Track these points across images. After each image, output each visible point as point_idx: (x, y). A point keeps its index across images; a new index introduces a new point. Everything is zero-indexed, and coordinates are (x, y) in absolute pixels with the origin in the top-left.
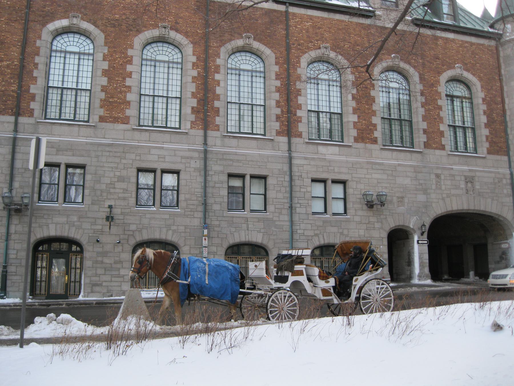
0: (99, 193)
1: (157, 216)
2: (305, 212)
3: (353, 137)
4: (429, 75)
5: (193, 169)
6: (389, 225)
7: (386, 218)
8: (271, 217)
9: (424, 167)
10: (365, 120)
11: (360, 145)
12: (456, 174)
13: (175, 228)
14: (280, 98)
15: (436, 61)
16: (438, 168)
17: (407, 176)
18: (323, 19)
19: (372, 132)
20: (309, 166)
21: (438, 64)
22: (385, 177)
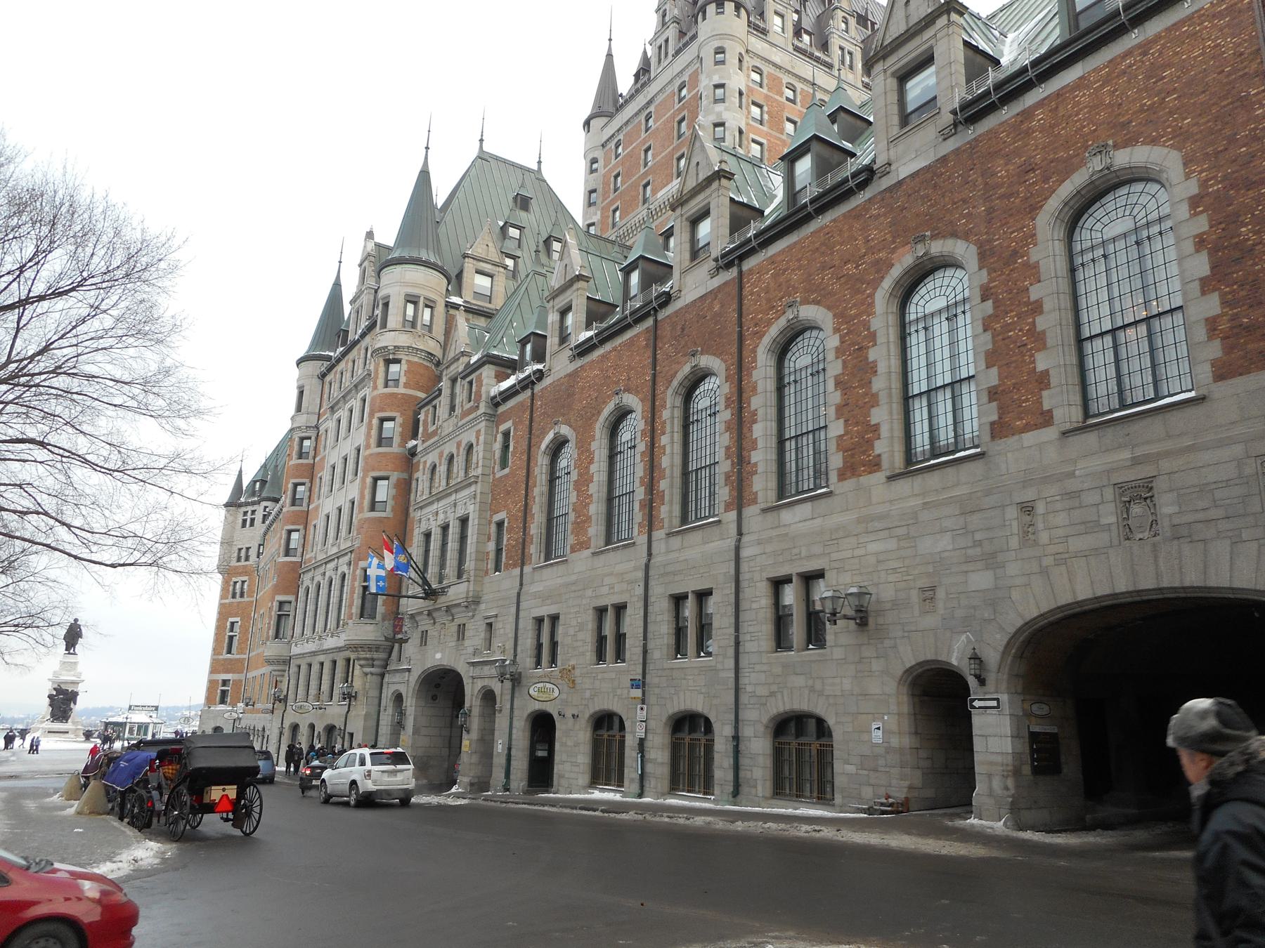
0: (566, 649)
1: (606, 675)
4: (1005, 233)
6: (903, 662)
7: (895, 647)
8: (713, 664)
9: (988, 493)
10: (857, 424)
11: (850, 484)
12: (1086, 486)
13: (619, 692)
15: (1025, 182)
16: (1026, 484)
17: (943, 531)
18: (790, 247)
19: (870, 444)
22: (892, 544)
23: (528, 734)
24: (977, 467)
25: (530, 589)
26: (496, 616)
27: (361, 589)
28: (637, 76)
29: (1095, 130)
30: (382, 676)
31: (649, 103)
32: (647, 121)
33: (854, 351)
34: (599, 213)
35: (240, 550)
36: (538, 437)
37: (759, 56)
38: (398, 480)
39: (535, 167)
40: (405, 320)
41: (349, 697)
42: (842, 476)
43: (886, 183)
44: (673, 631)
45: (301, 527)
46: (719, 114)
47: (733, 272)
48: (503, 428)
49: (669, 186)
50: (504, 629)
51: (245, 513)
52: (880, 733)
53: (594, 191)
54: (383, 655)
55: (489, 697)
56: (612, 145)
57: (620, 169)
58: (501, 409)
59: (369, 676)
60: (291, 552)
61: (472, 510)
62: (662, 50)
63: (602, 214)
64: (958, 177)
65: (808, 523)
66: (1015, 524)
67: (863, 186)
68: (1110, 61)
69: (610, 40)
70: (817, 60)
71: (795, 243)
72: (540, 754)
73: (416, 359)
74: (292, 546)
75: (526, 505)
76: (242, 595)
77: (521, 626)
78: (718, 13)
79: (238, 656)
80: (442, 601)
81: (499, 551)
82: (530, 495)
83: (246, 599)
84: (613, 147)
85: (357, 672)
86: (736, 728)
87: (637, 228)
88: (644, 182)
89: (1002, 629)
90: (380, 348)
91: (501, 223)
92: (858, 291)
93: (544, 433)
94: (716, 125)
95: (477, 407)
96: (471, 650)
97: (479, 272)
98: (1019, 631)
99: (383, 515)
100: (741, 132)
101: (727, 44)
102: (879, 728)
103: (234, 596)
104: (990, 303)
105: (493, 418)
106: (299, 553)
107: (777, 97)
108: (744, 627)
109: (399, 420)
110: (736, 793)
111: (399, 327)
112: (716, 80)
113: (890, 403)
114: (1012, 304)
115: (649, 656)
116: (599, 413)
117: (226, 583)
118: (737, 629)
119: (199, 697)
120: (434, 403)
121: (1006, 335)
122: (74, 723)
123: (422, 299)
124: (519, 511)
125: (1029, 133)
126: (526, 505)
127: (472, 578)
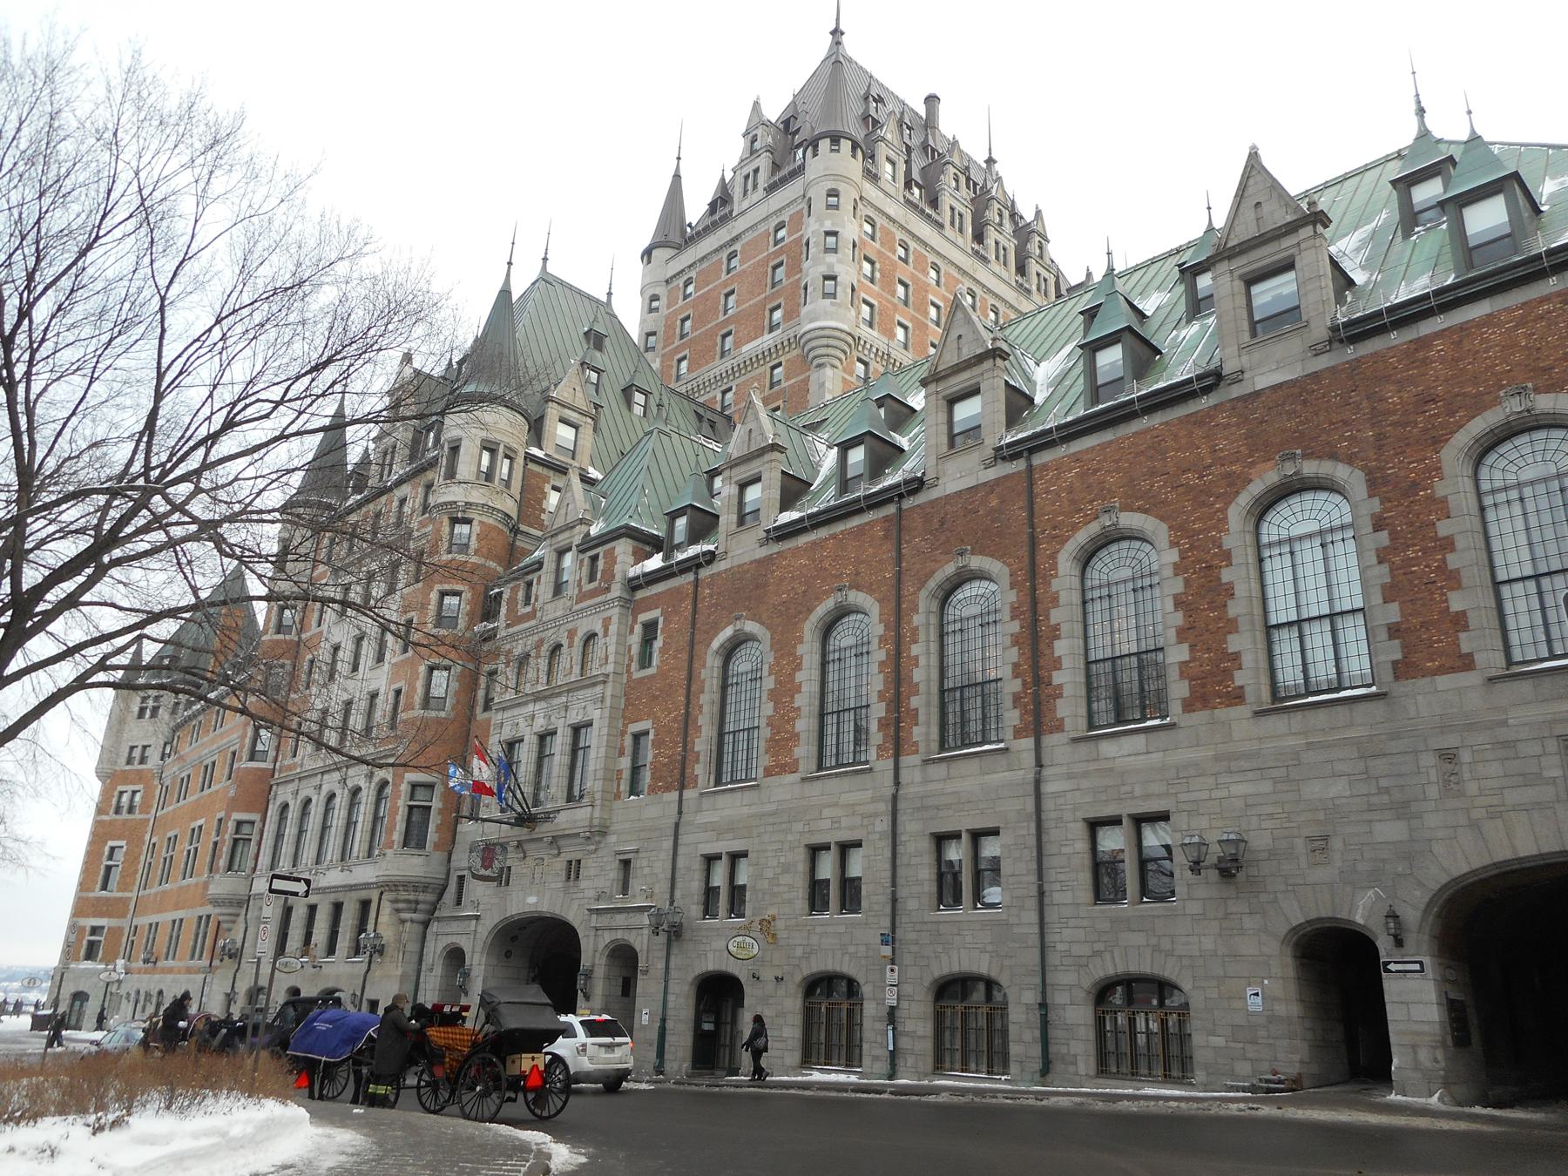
0: (760, 895)
1: (830, 929)
2: (1070, 901)
3: (1179, 702)
4: (1401, 462)
5: (877, 836)
7: (1275, 901)
8: (1004, 917)
9: (1395, 736)
10: (1209, 650)
11: (1200, 717)
13: (851, 949)
14: (1020, 655)
18: (1103, 447)
19: (1228, 674)
20: (1078, 793)
21: (1431, 416)
22: (1266, 787)
23: (692, 1001)
24: (1377, 708)
26: (637, 851)
27: (406, 809)
28: (713, 207)
29: (1509, 371)
30: (426, 924)
32: (729, 260)
33: (1200, 568)
34: (658, 360)
35: (132, 748)
36: (706, 632)
37: (873, 205)
39: (604, 299)
40: (479, 471)
42: (1188, 706)
43: (1236, 391)
44: (934, 877)
46: (830, 266)
47: (1019, 465)
48: (644, 617)
49: (759, 341)
51: (144, 699)
52: (1259, 1000)
53: (654, 334)
54: (430, 897)
55: (624, 958)
57: (690, 312)
58: (640, 595)
59: (408, 924)
60: (258, 756)
61: (596, 715)
62: (750, 179)
63: (662, 362)
64: (1335, 397)
65: (1141, 757)
66: (1433, 772)
67: (1207, 390)
68: (1524, 304)
69: (679, 158)
70: (929, 216)
71: (1111, 442)
72: (707, 1027)
73: (491, 521)
74: (260, 747)
75: (687, 714)
76: (131, 810)
77: (681, 863)
78: (832, 151)
79: (120, 895)
80: (544, 829)
81: (636, 770)
82: (693, 702)
83: (137, 816)
84: (681, 285)
85: (383, 918)
86: (1044, 993)
87: (711, 385)
88: (724, 331)
89: (1421, 884)
92: (1203, 504)
93: (716, 629)
94: (826, 278)
95: (608, 590)
96: (592, 893)
97: (563, 421)
98: (1445, 887)
100: (853, 289)
101: (842, 187)
102: (1257, 994)
104: (1385, 533)
105: (631, 606)
107: (890, 254)
108: (1050, 875)
109: (467, 595)
110: (1046, 1070)
111: (472, 478)
112: (828, 226)
114: (1414, 538)
115: (899, 906)
116: (810, 611)
117: (106, 794)
118: (1040, 877)
120: (529, 577)
121: (1408, 570)
123: (502, 446)
124: (675, 720)
125: (1426, 362)
126: (687, 714)
127: (598, 802)
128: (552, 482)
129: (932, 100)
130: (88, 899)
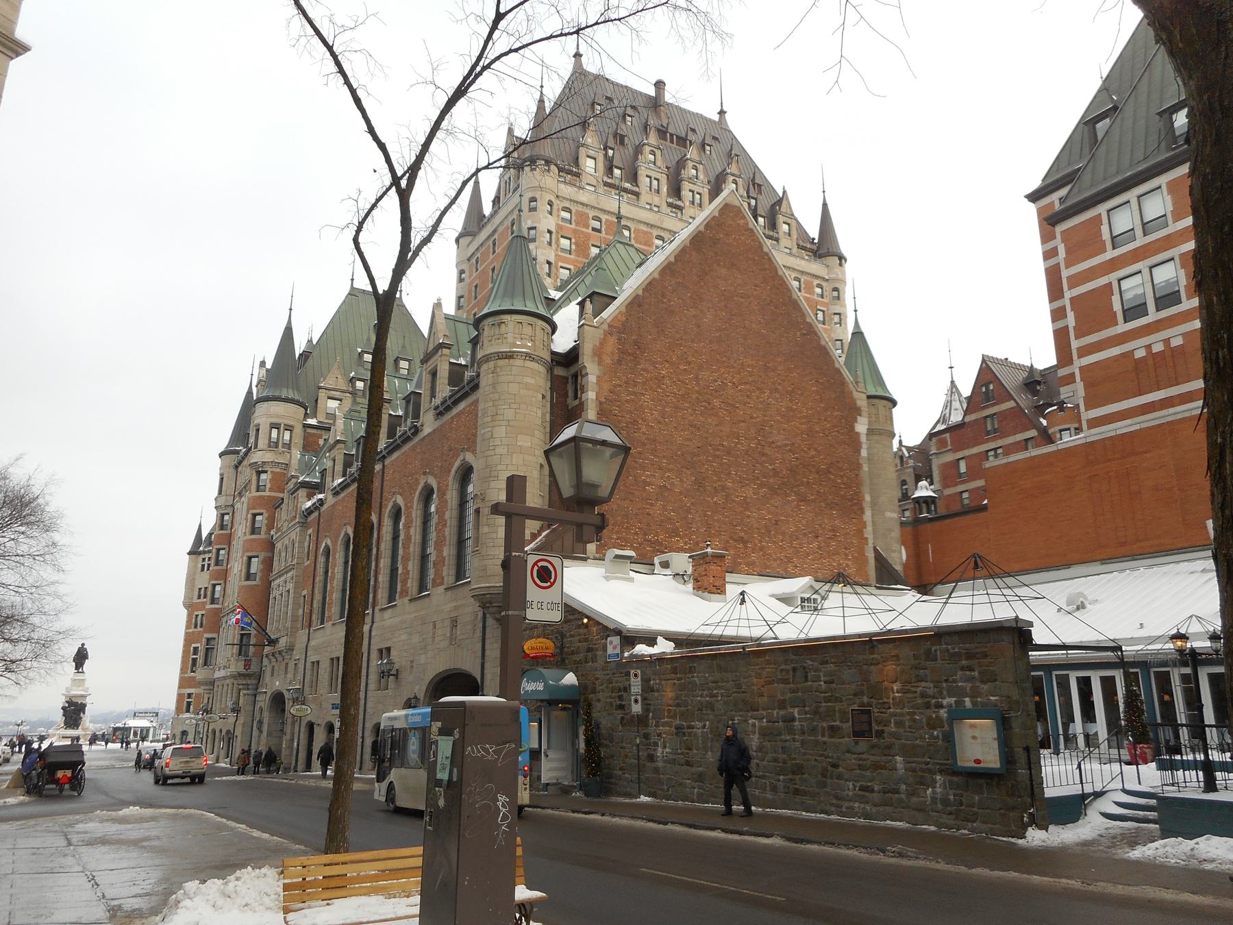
25: (312, 643)
28: (494, 202)
31: (495, 231)
35: (200, 589)
38: (264, 558)
41: (236, 710)
45: (222, 582)
50: (301, 666)
51: (204, 560)
53: (462, 297)
54: (255, 682)
56: (474, 261)
73: (278, 470)
74: (217, 596)
90: (253, 463)
91: (359, 350)
99: (254, 583)
103: (196, 627)
105: (304, 525)
106: (221, 602)
107: (584, 230)
109: (266, 515)
111: (266, 447)
113: (414, 560)
117: (189, 616)
119: (173, 706)
122: (83, 729)
128: (324, 437)
129: (660, 85)
130: (185, 678)
